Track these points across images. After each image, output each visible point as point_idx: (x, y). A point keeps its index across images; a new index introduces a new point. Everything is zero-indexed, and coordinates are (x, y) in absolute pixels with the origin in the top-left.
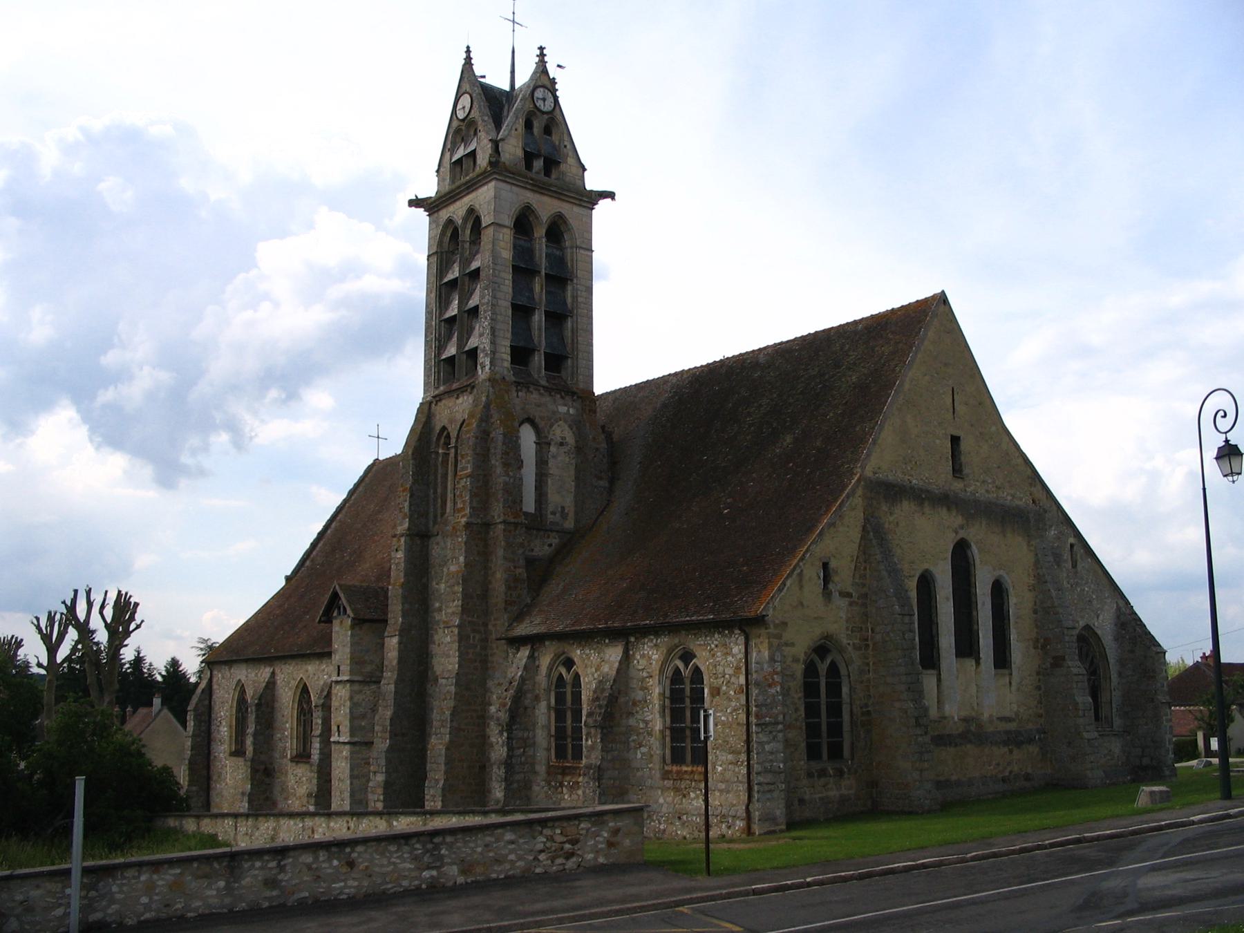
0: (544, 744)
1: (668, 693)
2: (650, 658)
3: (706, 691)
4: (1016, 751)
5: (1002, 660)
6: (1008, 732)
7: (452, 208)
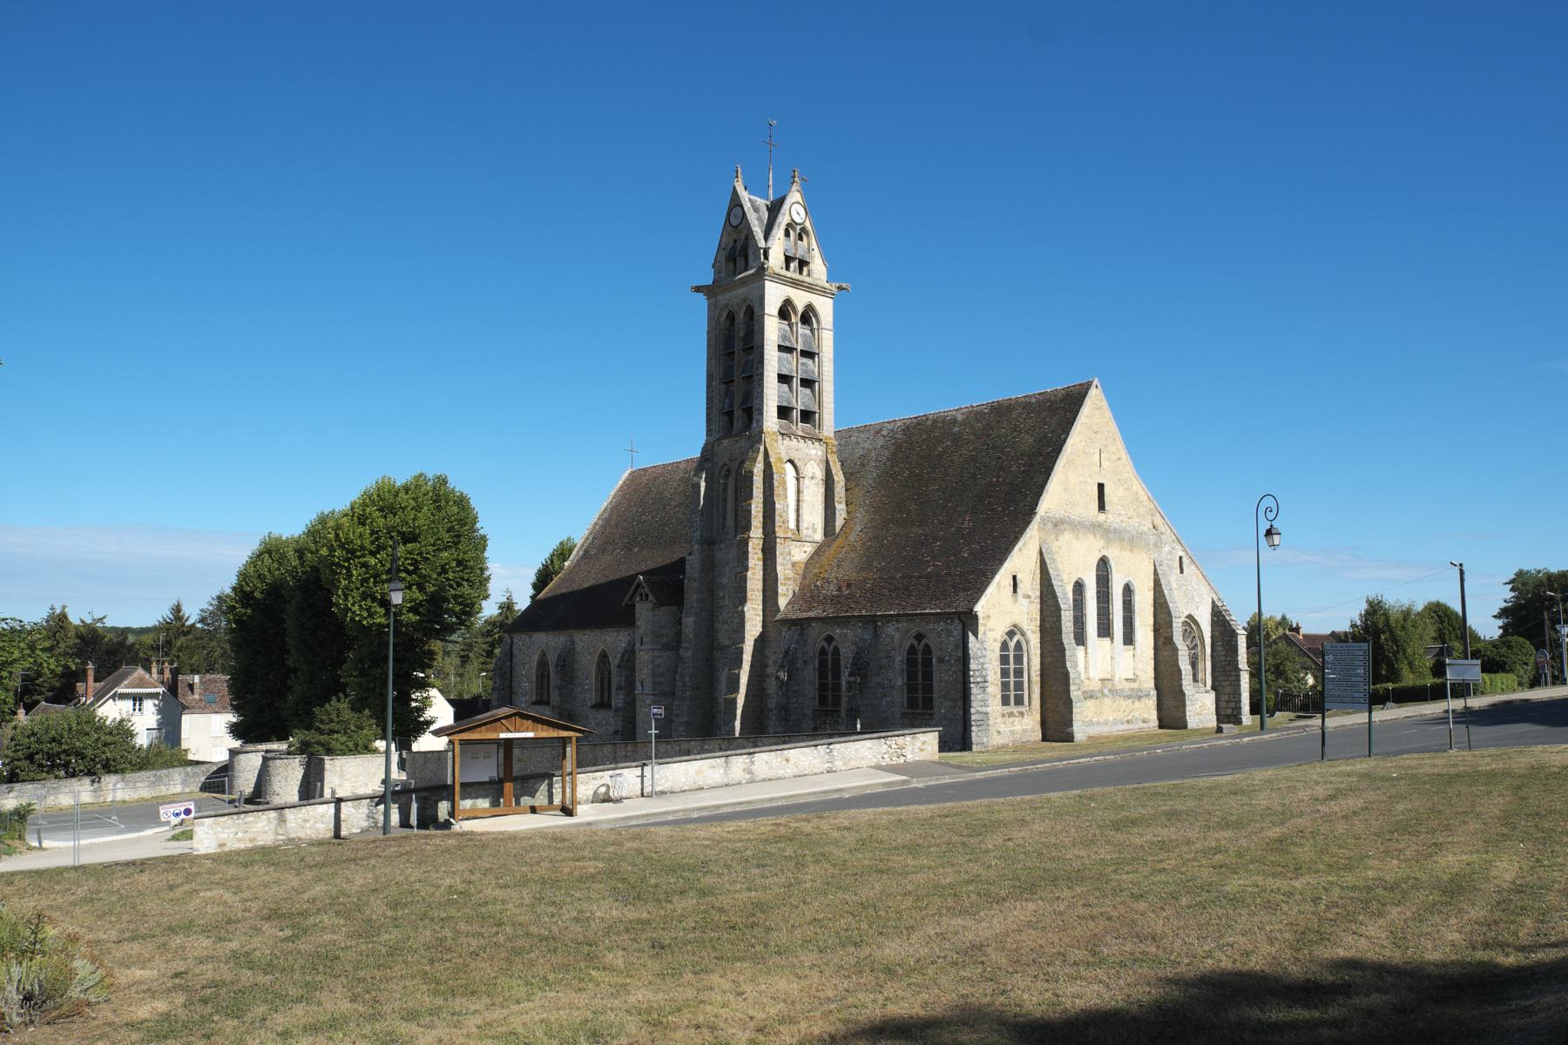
5: (1129, 639)
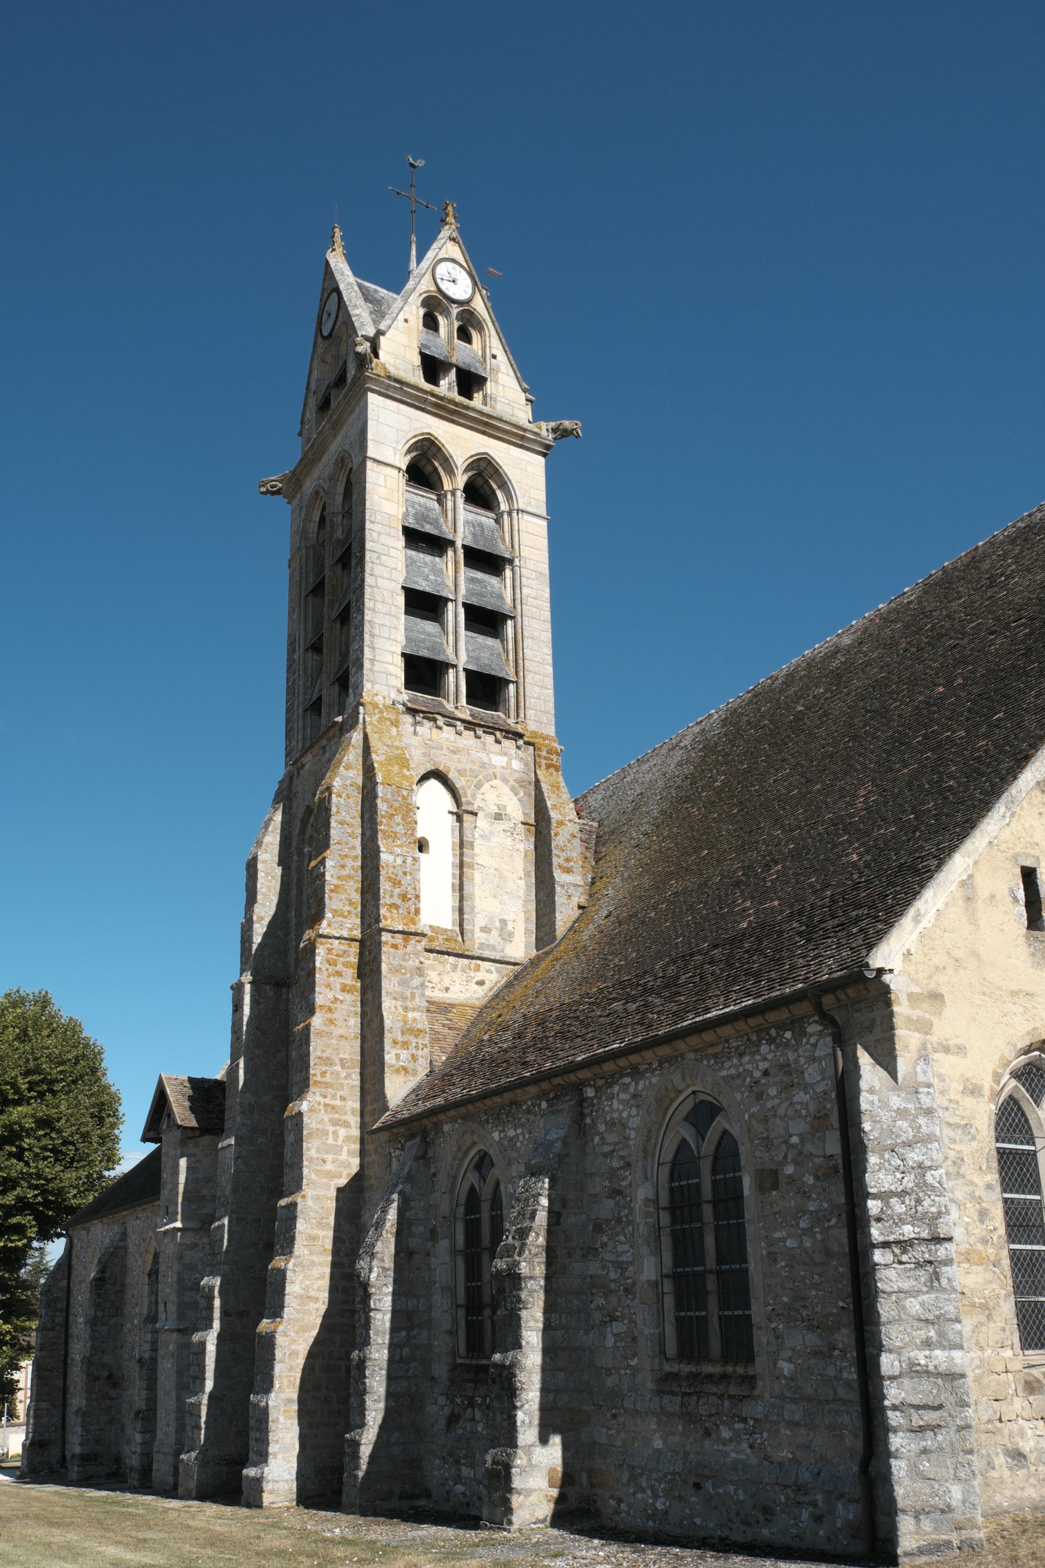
0: (447, 1325)
1: (664, 1200)
2: (624, 1125)
3: (747, 1182)
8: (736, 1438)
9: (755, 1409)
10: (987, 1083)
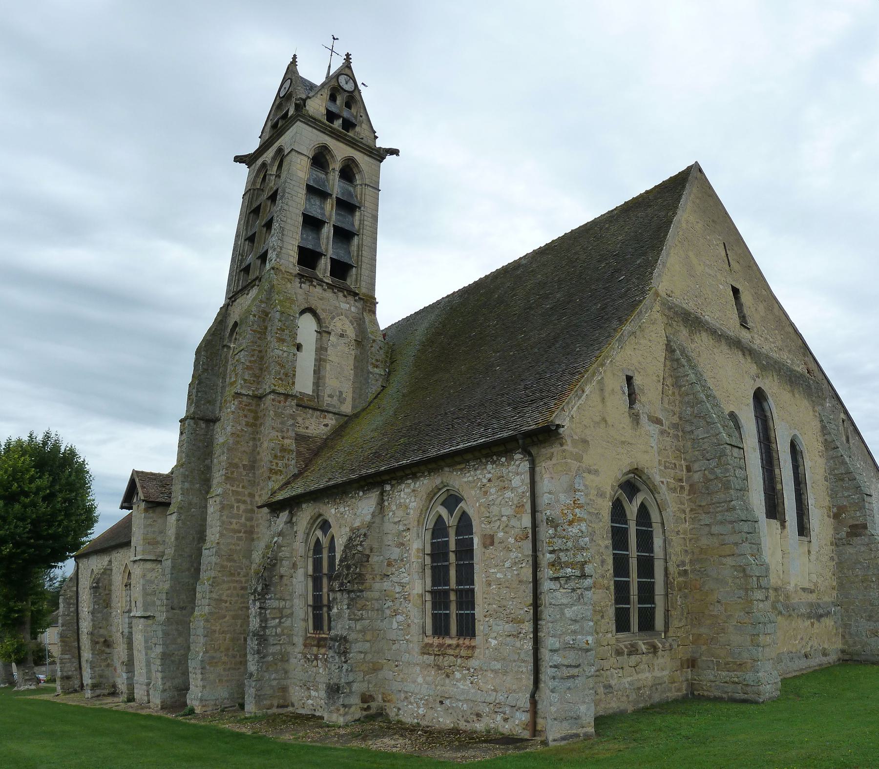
0: (302, 614)
1: (428, 550)
2: (407, 507)
3: (476, 541)
4: (816, 624)
6: (811, 605)
7: (265, 155)
8: (464, 678)
9: (473, 663)
10: (609, 491)
